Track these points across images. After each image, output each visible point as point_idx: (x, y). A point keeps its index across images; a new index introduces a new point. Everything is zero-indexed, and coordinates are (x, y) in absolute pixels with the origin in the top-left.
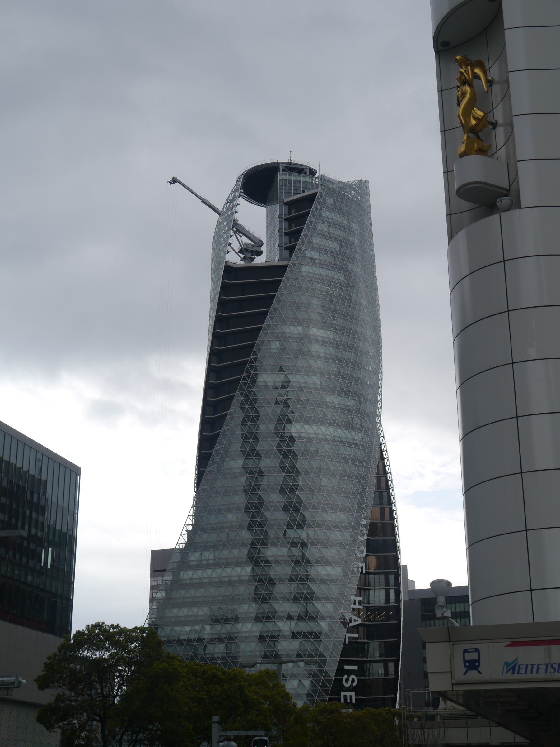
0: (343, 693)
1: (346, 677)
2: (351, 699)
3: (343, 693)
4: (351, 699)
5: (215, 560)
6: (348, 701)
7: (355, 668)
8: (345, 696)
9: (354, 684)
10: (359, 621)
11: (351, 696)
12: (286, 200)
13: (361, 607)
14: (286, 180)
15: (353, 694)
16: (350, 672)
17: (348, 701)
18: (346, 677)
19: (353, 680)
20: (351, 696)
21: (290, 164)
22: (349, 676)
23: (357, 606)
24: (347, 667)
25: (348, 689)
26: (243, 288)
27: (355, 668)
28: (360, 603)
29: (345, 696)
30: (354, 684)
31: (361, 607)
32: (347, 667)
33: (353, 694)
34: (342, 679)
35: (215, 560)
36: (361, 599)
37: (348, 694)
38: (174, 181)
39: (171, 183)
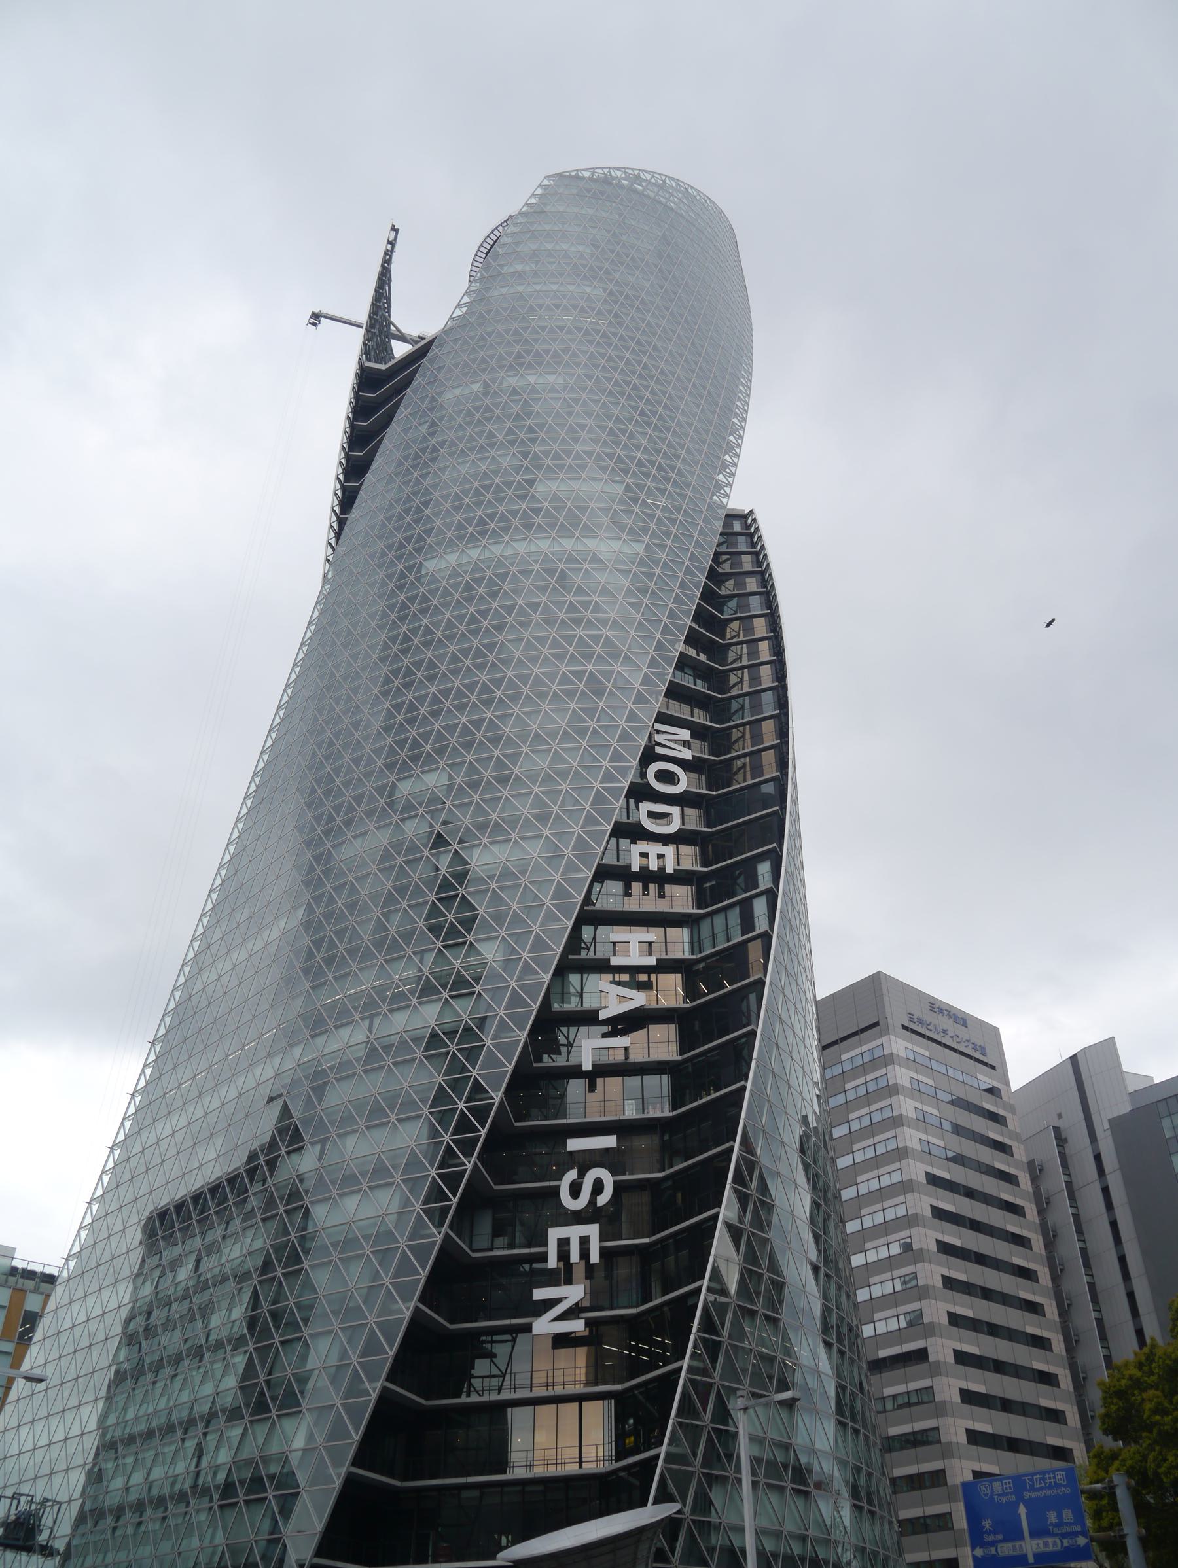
0: (555, 1234)
1: (572, 1175)
2: (585, 1254)
3: (555, 1234)
4: (585, 1254)
6: (575, 1256)
7: (610, 1141)
8: (564, 1243)
9: (603, 1200)
10: (639, 999)
11: (584, 1241)
13: (651, 961)
15: (592, 1230)
16: (585, 1161)
17: (575, 1256)
18: (572, 1175)
19: (598, 1187)
20: (584, 1241)
22: (582, 1175)
24: (574, 1144)
25: (578, 1218)
27: (610, 1141)
29: (564, 1243)
30: (603, 1200)
32: (574, 1144)
33: (592, 1230)
37: (574, 1233)
38: (316, 317)
39: (314, 324)
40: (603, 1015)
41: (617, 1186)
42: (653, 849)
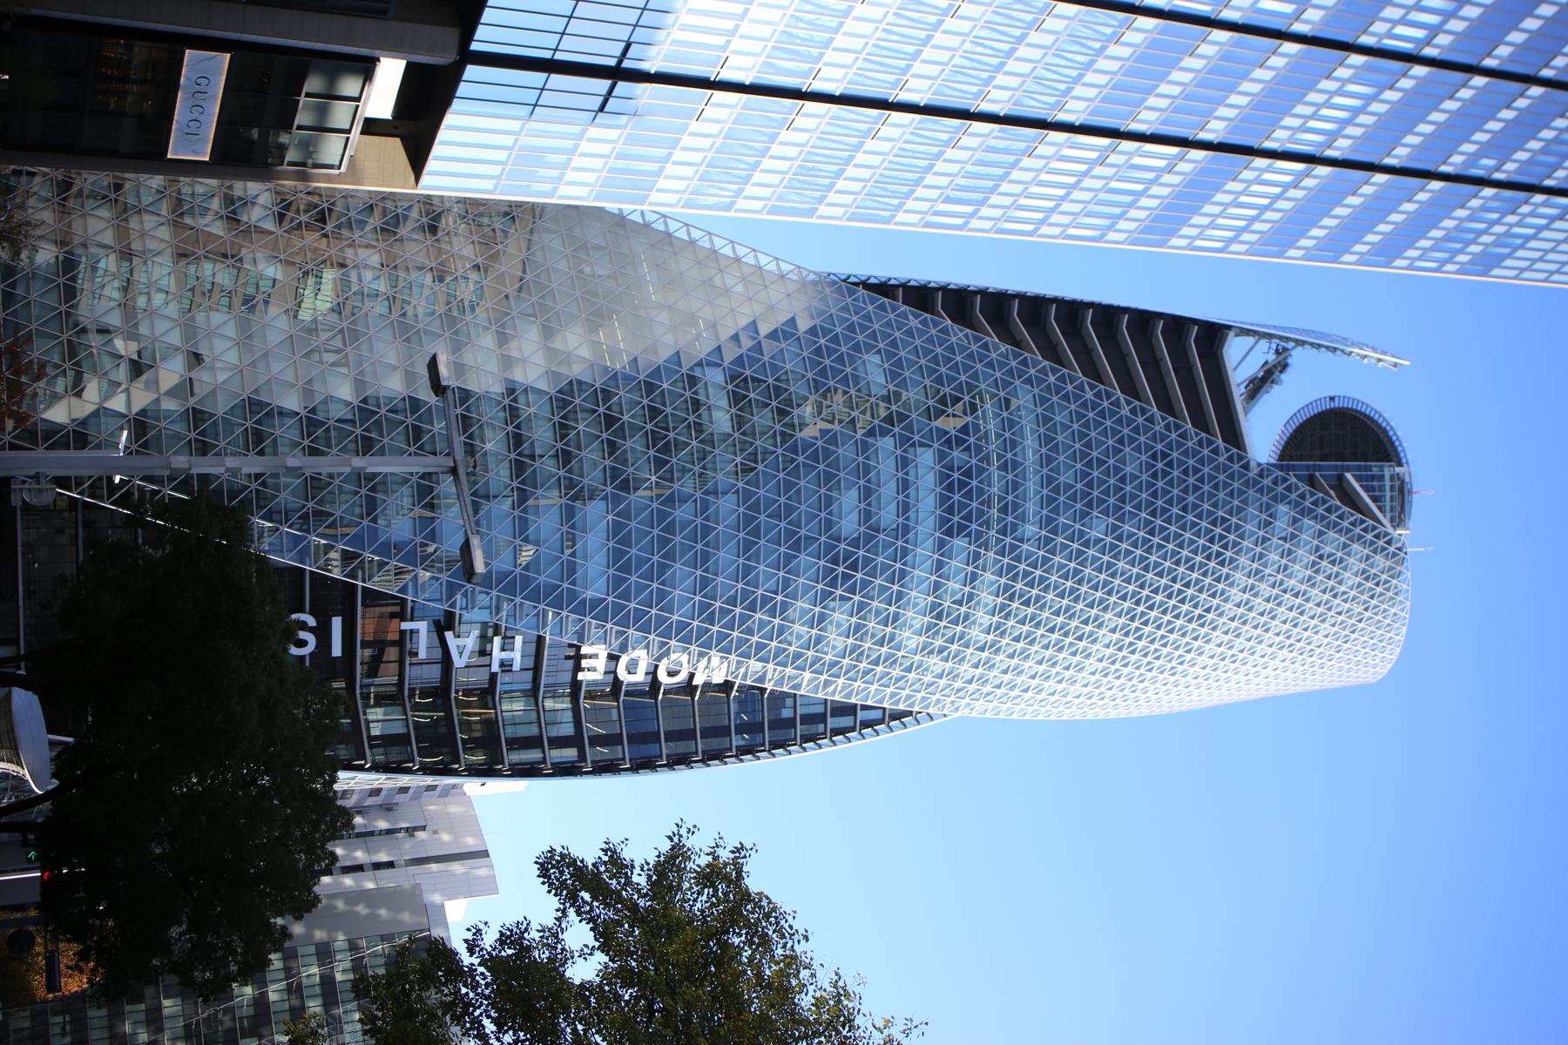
1: (312, 622)
5: (593, 276)
7: (337, 651)
10: (459, 662)
12: (1349, 476)
14: (1382, 478)
16: (323, 633)
18: (312, 622)
21: (1410, 492)
22: (311, 630)
23: (497, 655)
24: (337, 623)
26: (1185, 371)
27: (337, 651)
28: (506, 666)
31: (495, 668)
32: (337, 623)
34: (302, 611)
35: (593, 276)
36: (516, 667)
40: (449, 635)
41: (302, 658)
42: (601, 664)
